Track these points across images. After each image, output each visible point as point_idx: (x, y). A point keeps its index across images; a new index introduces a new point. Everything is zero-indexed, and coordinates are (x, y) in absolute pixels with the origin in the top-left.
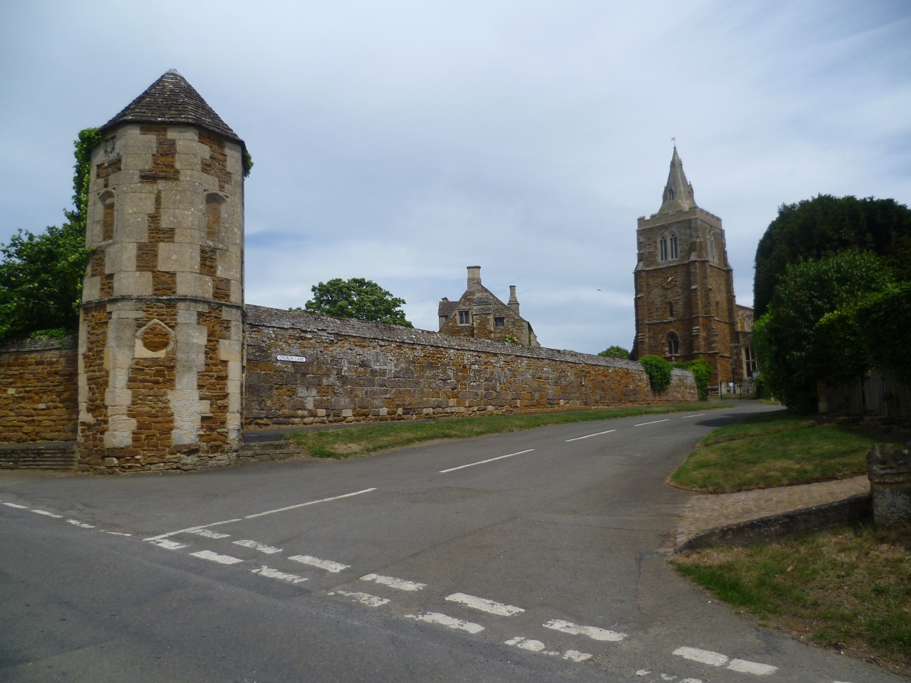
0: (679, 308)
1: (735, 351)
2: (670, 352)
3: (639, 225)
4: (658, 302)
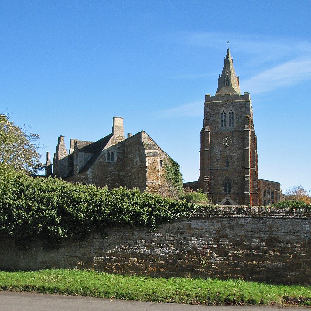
2: (225, 190)
3: (206, 100)
4: (218, 156)
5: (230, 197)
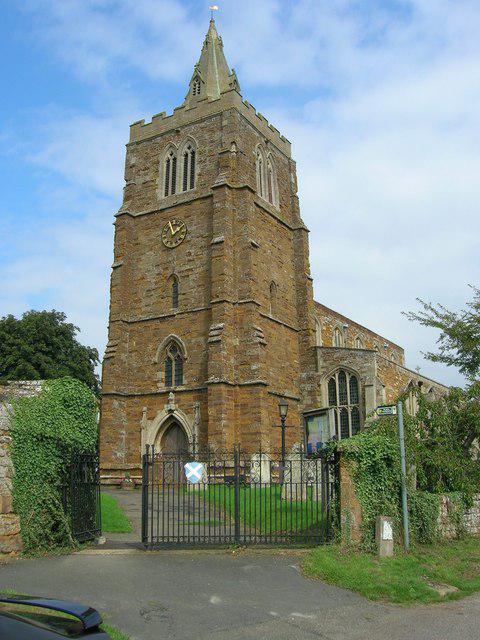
0: (192, 290)
1: (308, 387)
2: (168, 383)
3: (133, 135)
4: (151, 278)
5: (177, 401)
